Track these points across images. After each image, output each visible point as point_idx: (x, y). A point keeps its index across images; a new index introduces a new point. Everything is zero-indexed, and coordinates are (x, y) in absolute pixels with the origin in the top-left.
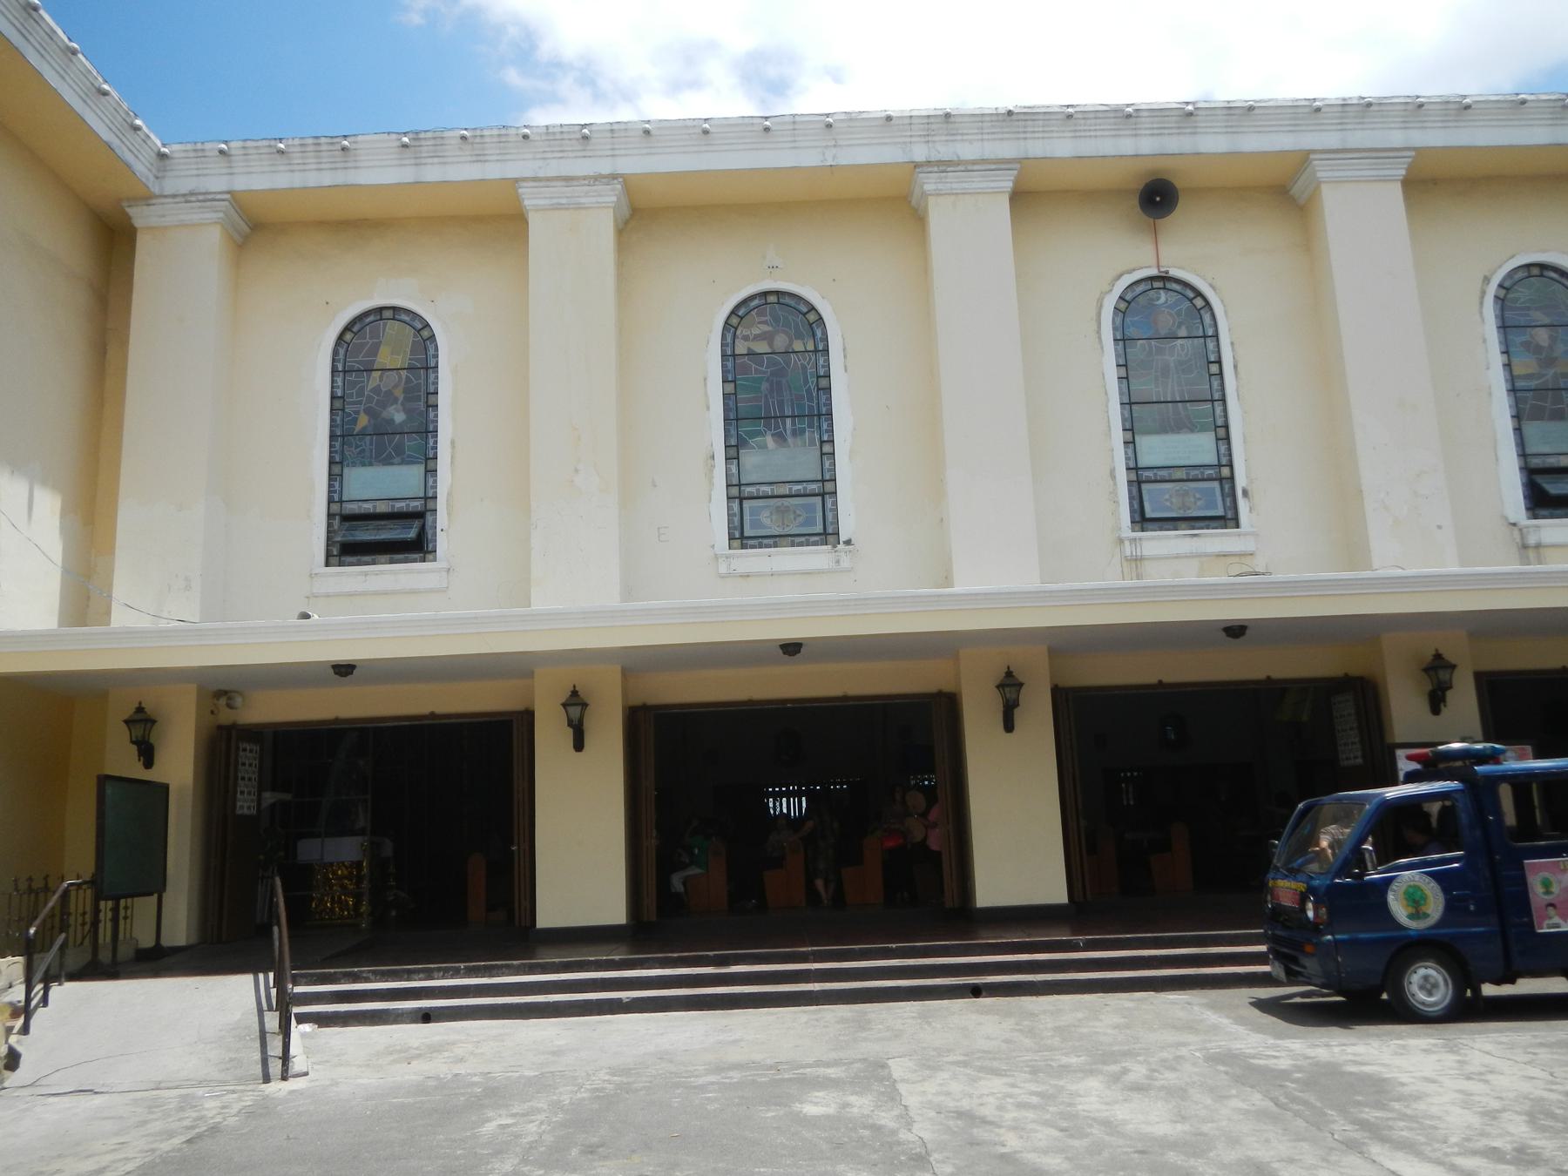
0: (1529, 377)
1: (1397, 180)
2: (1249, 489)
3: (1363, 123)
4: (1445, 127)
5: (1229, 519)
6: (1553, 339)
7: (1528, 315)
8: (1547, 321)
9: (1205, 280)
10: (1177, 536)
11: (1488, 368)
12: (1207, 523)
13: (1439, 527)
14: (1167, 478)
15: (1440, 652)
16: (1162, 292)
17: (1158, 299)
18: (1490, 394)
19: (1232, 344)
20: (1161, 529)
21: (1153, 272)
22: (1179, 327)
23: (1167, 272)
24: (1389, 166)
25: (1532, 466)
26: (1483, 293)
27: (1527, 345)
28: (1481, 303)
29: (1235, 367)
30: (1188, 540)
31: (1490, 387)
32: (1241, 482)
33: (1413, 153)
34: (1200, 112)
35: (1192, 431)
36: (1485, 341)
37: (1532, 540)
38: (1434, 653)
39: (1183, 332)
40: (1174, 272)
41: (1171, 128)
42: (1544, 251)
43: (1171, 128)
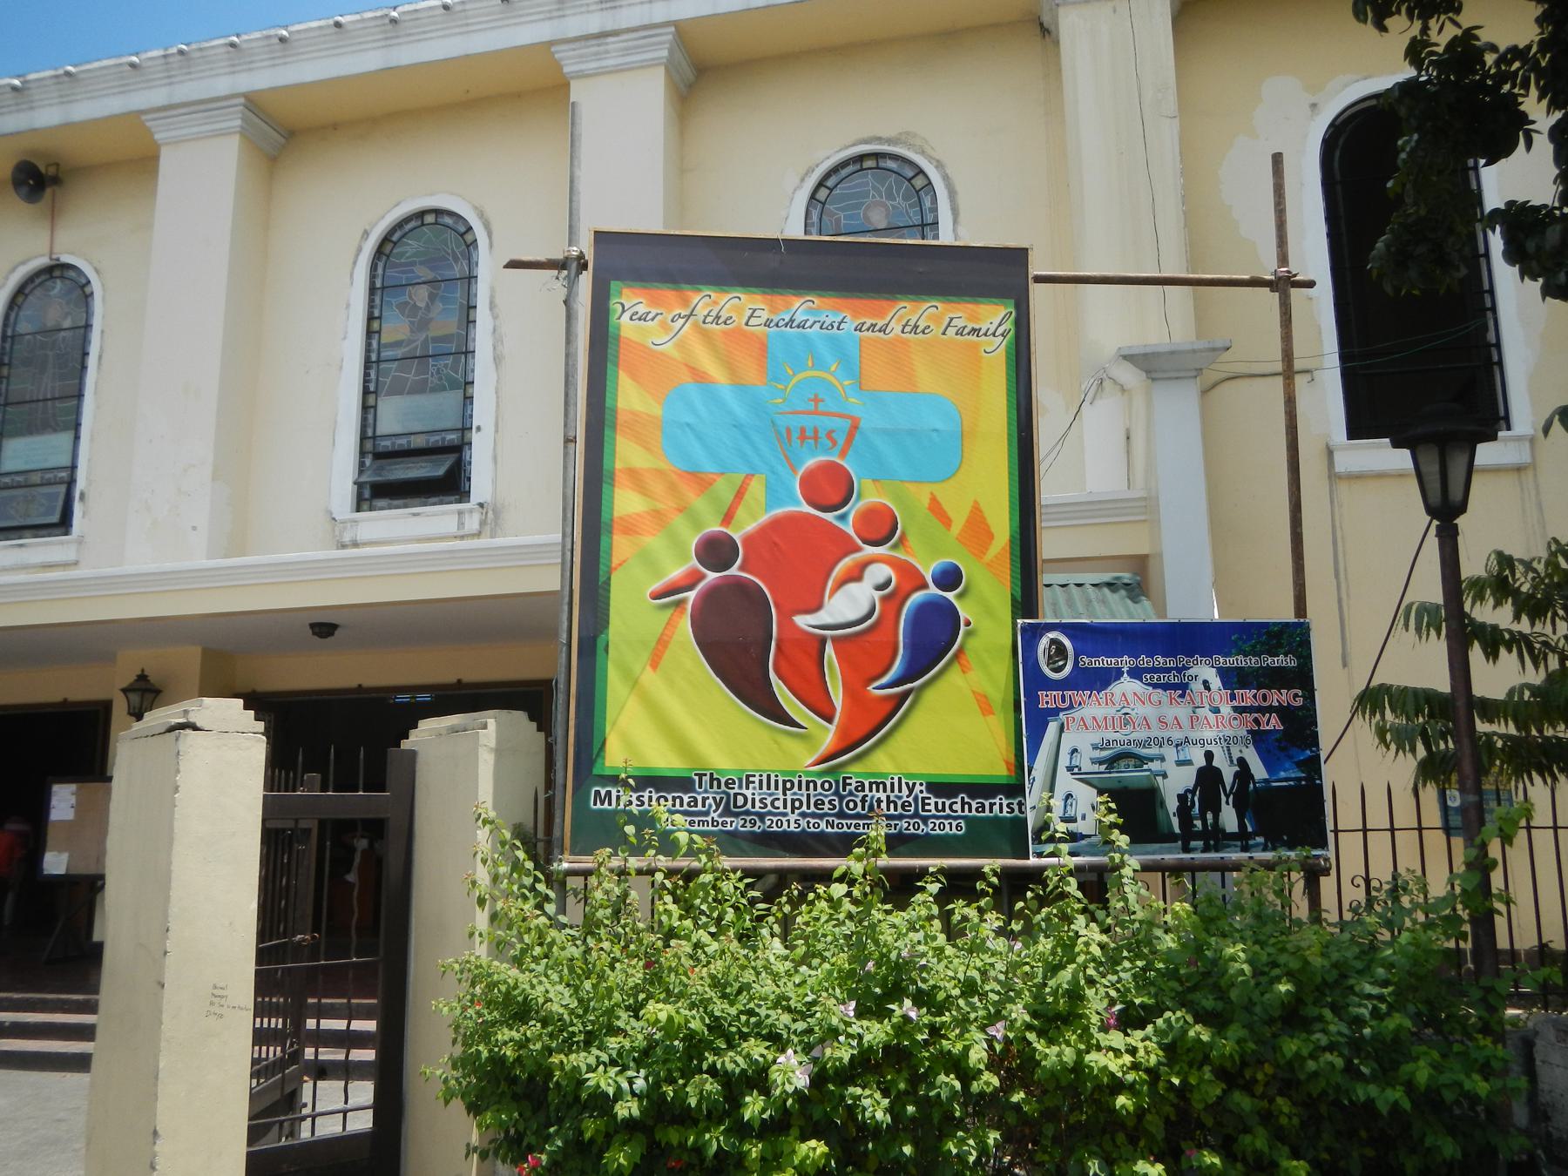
0: (397, 344)
1: (235, 133)
2: (86, 491)
3: (190, 73)
4: (274, 65)
5: (64, 524)
6: (432, 297)
7: (413, 272)
8: (430, 275)
9: (91, 263)
10: (6, 547)
11: (345, 338)
12: (50, 531)
13: (194, 528)
14: (23, 484)
15: (146, 673)
16: (58, 281)
17: (54, 288)
18: (341, 367)
19: (102, 332)
20: (50, 535)
21: (43, 261)
22: (65, 317)
23: (58, 260)
24: (222, 118)
25: (381, 450)
26: (359, 250)
27: (402, 307)
28: (355, 263)
29: (100, 357)
30: (17, 550)
31: (342, 360)
32: (81, 484)
33: (242, 100)
34: (31, 85)
35: (55, 431)
36: (348, 306)
37: (347, 538)
38: (140, 673)
39: (67, 324)
40: (66, 259)
41: (9, 106)
42: (432, 195)
43: (9, 106)
